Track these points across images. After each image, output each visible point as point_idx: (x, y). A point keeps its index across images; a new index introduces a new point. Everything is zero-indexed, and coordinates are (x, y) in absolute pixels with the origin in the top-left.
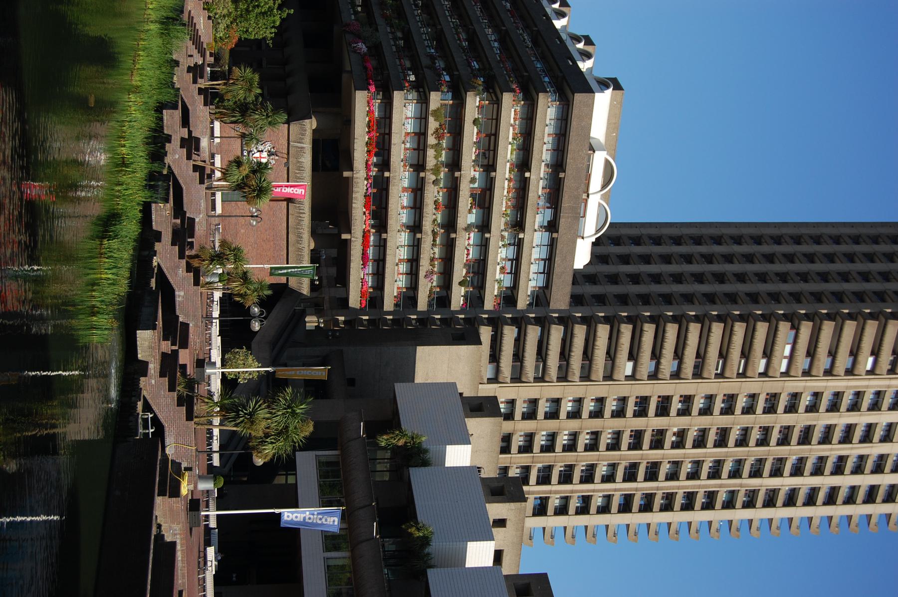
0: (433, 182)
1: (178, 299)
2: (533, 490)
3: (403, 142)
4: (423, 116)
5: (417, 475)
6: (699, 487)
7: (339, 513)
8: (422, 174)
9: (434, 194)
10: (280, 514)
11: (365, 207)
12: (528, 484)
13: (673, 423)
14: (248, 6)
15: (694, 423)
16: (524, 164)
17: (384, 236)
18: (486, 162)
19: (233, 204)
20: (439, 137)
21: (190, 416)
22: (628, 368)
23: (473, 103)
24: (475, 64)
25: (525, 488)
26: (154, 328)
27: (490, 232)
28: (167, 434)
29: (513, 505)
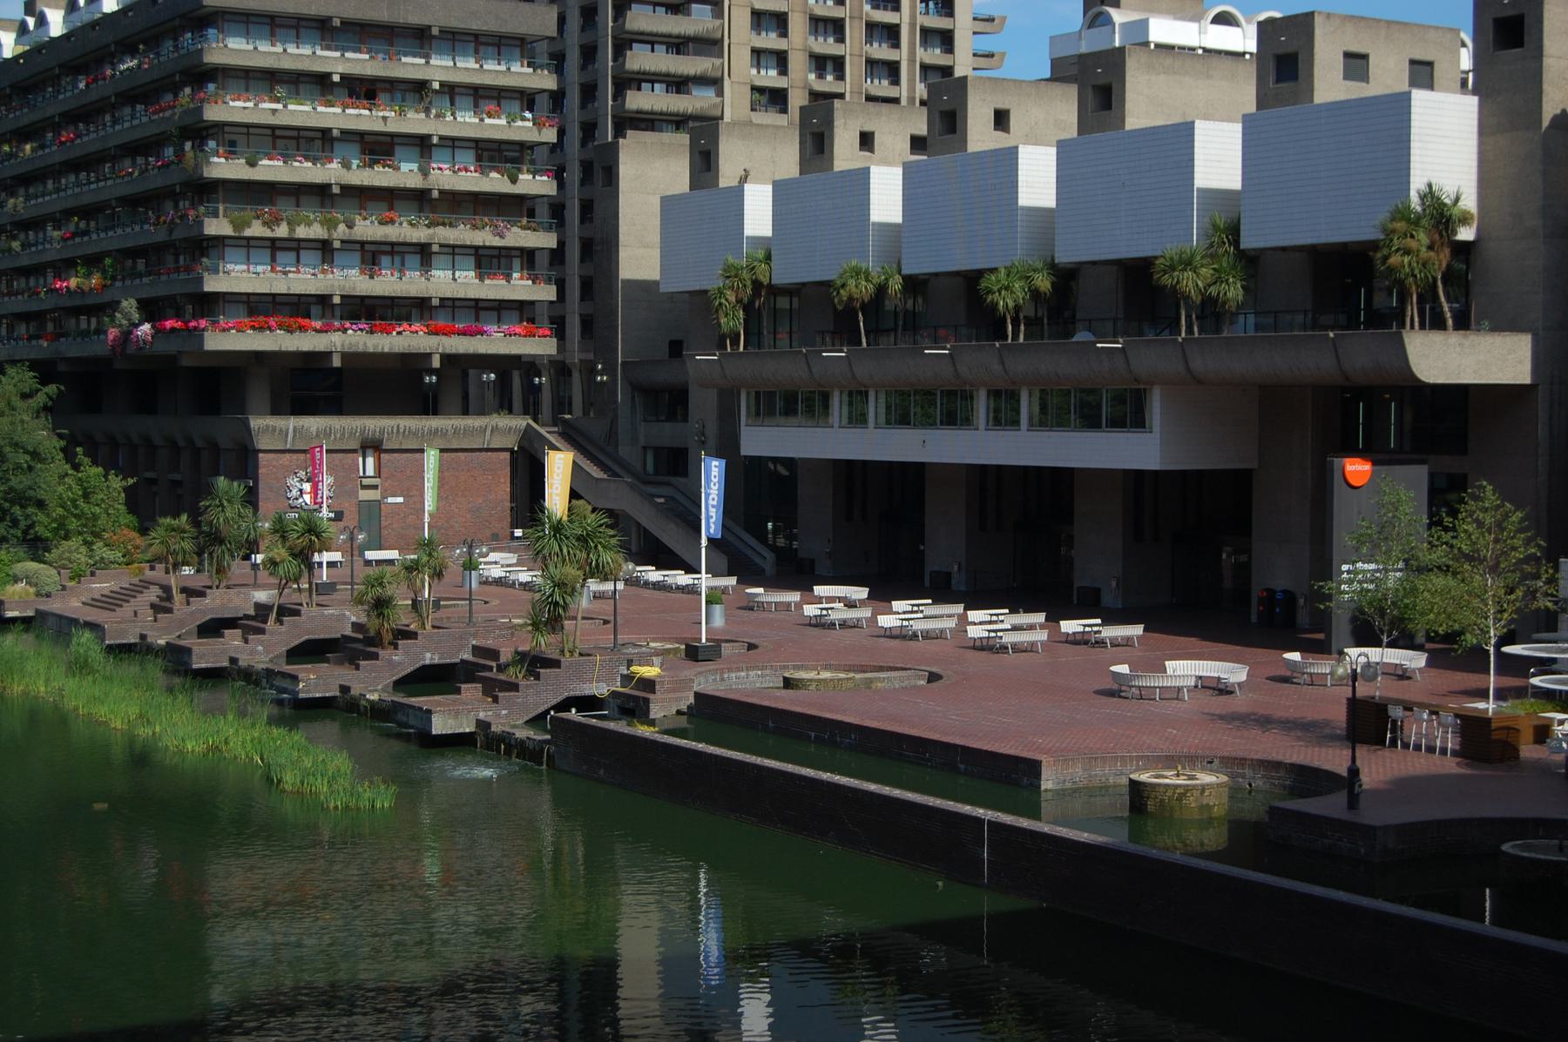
0: (350, 226)
1: (436, 661)
3: (285, 273)
4: (244, 243)
5: (783, 274)
7: (708, 459)
8: (337, 245)
9: (368, 228)
10: (710, 540)
14: (75, 516)
16: (319, 84)
17: (435, 302)
18: (318, 143)
19: (384, 532)
20: (277, 221)
21: (555, 664)
23: (222, 167)
24: (169, 152)
26: (429, 712)
27: (430, 136)
28: (578, 693)
29: (839, 123)
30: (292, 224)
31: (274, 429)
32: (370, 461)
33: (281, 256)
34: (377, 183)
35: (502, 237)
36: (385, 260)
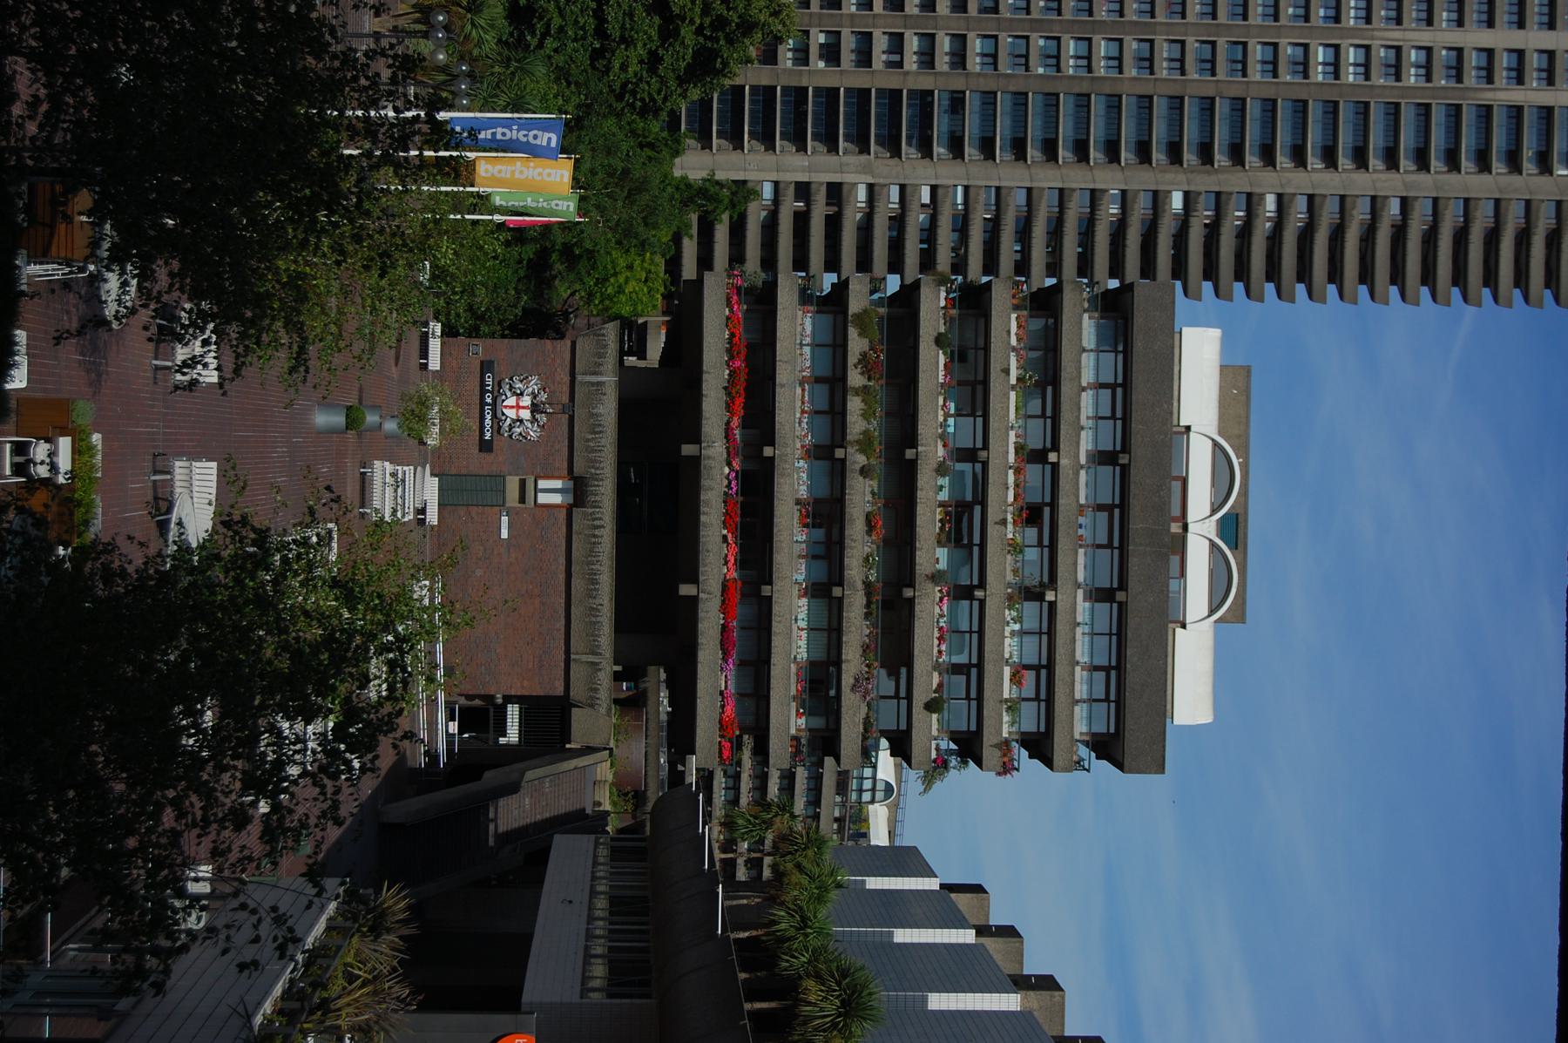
9: (862, 496)
11: (725, 524)
19: (462, 511)
30: (864, 391)
31: (601, 356)
32: (556, 499)
33: (829, 351)
34: (920, 509)
35: (854, 688)
36: (820, 534)
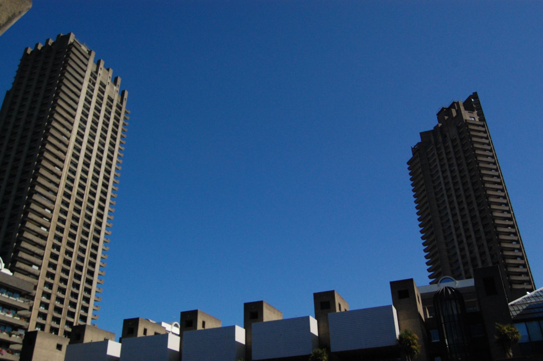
2: (76, 321)
6: (89, 250)
12: (73, 323)
13: (62, 255)
15: (64, 246)
22: (36, 268)
25: (74, 325)
29: (140, 324)
